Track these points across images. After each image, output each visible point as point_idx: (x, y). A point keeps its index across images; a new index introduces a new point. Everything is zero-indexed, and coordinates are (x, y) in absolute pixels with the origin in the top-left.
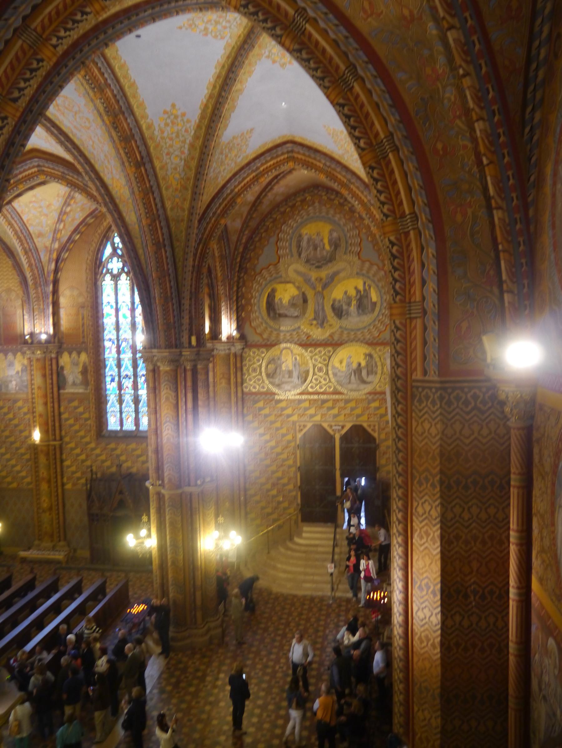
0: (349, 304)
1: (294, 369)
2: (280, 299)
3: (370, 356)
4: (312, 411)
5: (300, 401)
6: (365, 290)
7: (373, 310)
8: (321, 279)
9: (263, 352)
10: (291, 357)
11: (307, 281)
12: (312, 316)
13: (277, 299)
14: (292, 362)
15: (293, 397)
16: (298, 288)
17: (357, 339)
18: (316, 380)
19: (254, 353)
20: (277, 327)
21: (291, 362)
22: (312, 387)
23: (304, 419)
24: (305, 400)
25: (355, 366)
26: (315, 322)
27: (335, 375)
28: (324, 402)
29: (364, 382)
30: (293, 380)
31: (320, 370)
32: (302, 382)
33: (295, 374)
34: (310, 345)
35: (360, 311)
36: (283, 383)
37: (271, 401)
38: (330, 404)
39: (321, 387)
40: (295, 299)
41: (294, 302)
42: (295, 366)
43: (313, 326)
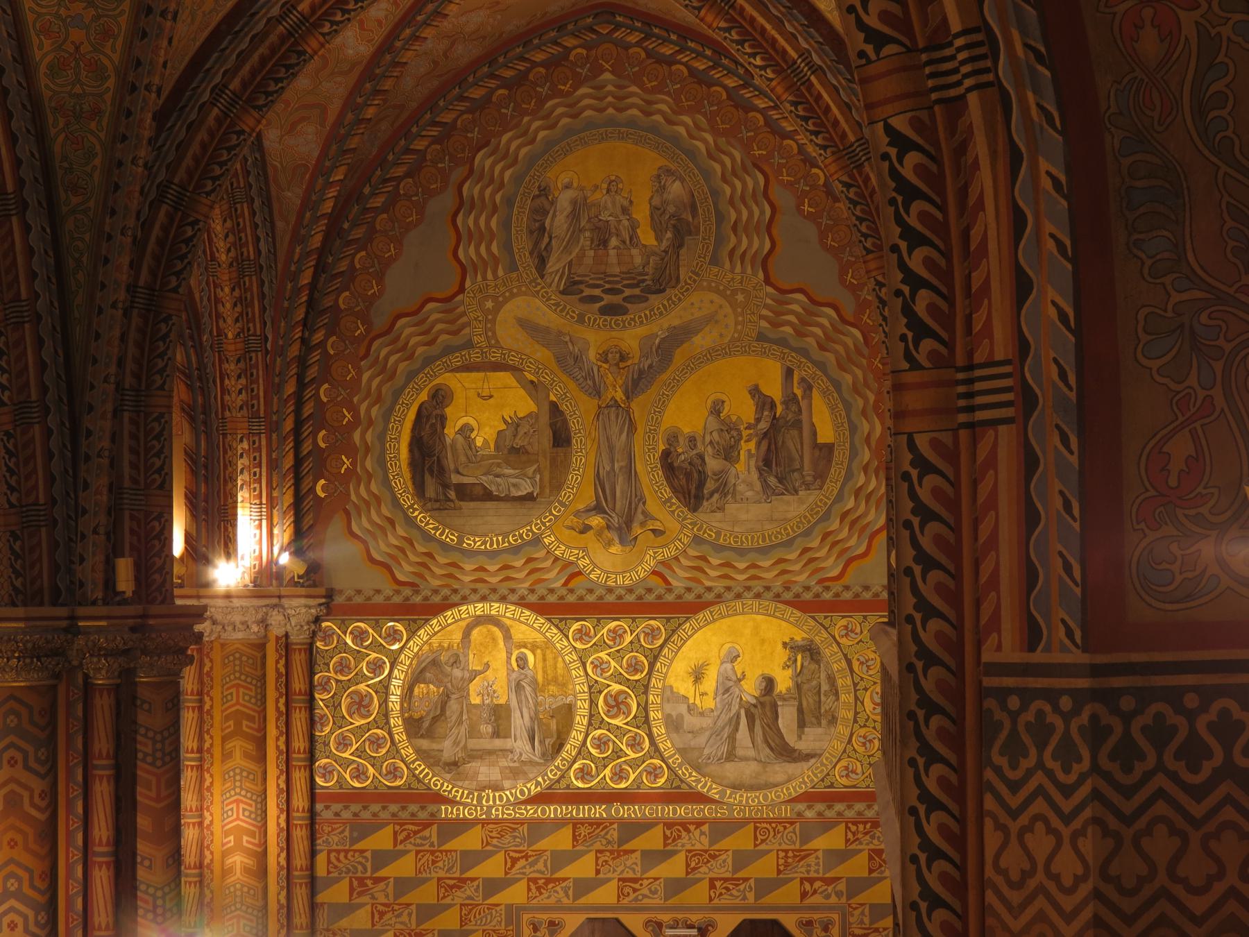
0: (729, 453)
1: (514, 703)
2: (465, 430)
3: (810, 651)
4: (583, 868)
5: (538, 828)
6: (791, 399)
7: (821, 477)
8: (623, 357)
9: (394, 636)
10: (504, 655)
11: (570, 361)
12: (588, 498)
13: (450, 432)
14: (510, 670)
15: (510, 813)
16: (533, 388)
17: (758, 587)
18: (601, 743)
19: (360, 636)
20: (451, 538)
21: (502, 674)
22: (584, 774)
23: (553, 900)
24: (559, 824)
25: (750, 689)
26: (596, 521)
27: (674, 724)
28: (633, 829)
29: (786, 753)
30: (509, 743)
31: (617, 704)
32: (543, 755)
33: (519, 722)
34: (580, 609)
35: (772, 481)
36: (475, 755)
37: (426, 825)
38: (653, 840)
39: (619, 775)
40: (522, 431)
41: (519, 442)
42: (519, 687)
43: (590, 534)
